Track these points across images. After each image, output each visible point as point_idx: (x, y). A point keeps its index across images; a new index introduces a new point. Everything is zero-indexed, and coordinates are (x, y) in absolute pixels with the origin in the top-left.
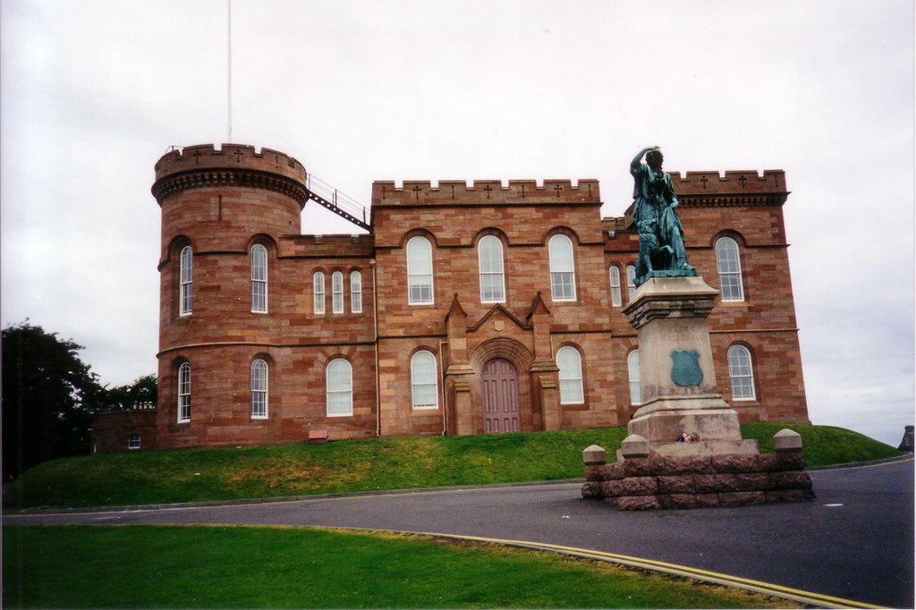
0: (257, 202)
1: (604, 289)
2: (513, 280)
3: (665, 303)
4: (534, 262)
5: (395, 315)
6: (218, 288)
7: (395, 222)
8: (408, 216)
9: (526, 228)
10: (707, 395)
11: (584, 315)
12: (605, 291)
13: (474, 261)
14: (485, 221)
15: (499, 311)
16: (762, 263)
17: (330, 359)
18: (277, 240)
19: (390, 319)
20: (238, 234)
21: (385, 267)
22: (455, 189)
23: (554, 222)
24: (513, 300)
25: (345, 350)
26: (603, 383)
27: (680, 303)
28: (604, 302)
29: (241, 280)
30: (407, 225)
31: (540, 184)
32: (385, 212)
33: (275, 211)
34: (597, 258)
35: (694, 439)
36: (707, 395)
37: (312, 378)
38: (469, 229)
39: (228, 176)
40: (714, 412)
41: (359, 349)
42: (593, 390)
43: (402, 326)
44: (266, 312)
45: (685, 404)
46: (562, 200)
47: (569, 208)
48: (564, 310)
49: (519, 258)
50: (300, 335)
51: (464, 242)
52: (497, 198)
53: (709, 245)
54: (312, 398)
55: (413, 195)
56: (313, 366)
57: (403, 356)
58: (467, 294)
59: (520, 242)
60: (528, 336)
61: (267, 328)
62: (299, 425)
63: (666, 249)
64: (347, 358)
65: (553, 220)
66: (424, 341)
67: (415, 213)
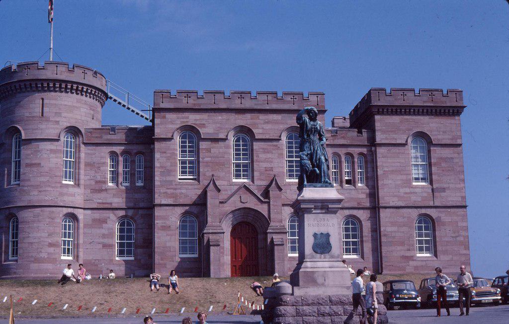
0: (70, 104)
2: (257, 165)
4: (274, 152)
6: (39, 164)
7: (170, 120)
9: (268, 127)
10: (333, 260)
16: (444, 156)
18: (83, 131)
33: (82, 110)
35: (323, 285)
36: (333, 260)
41: (141, 212)
44: (72, 183)
45: (320, 264)
51: (222, 136)
53: (404, 142)
54: (105, 246)
55: (185, 100)
56: (106, 223)
58: (222, 174)
60: (265, 206)
61: (73, 195)
63: (315, 170)
67: (186, 114)
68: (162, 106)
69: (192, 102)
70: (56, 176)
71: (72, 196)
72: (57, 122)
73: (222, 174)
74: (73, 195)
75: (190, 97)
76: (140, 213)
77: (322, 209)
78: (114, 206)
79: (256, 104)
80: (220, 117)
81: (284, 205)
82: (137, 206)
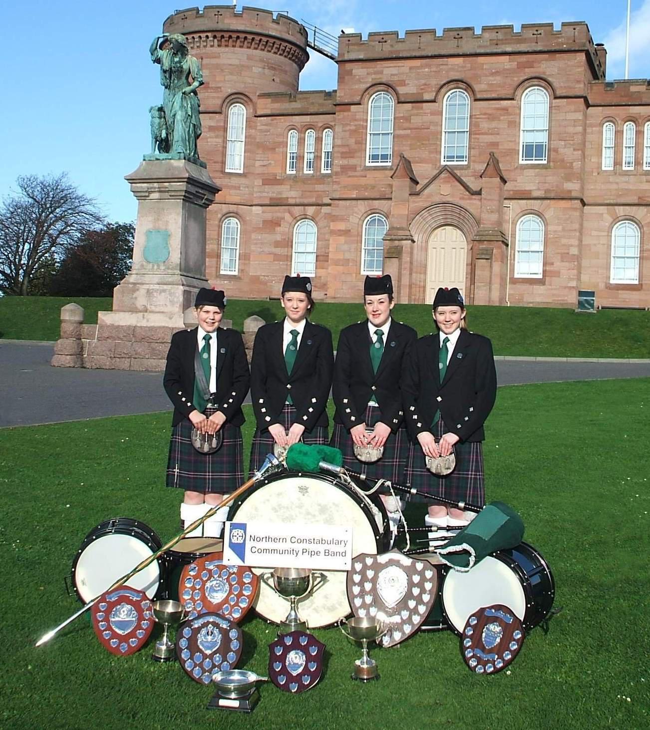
0: (236, 62)
1: (578, 150)
3: (145, 185)
4: (502, 118)
5: (350, 176)
7: (357, 77)
8: (371, 70)
9: (497, 80)
11: (552, 180)
12: (580, 152)
13: (435, 118)
14: (452, 73)
15: (452, 174)
17: (296, 219)
18: (254, 98)
19: (344, 180)
20: (214, 95)
21: (344, 125)
22: (423, 39)
23: (529, 72)
24: (474, 162)
25: (311, 210)
26: (565, 257)
27: (156, 185)
28: (577, 165)
29: (215, 139)
30: (370, 80)
31: (517, 29)
32: (348, 66)
33: (255, 70)
34: (573, 112)
37: (279, 238)
38: (435, 82)
39: (207, 37)
40: (165, 287)
42: (552, 264)
43: (356, 187)
44: (241, 172)
46: (539, 48)
47: (546, 56)
48: (531, 172)
49: (485, 114)
50: (270, 195)
51: (427, 97)
52: (468, 46)
54: (277, 258)
56: (280, 226)
57: (354, 220)
59: (485, 96)
61: (238, 188)
62: (265, 283)
64: (313, 219)
65: (526, 70)
66: (376, 203)
68: (346, 58)
69: (386, 49)
70: (215, 162)
71: (236, 189)
72: (218, 89)
73: (425, 154)
74: (238, 188)
75: (386, 42)
76: (322, 211)
77: (160, 191)
78: (291, 201)
79: (480, 47)
80: (426, 68)
81: (505, 199)
82: (320, 202)
